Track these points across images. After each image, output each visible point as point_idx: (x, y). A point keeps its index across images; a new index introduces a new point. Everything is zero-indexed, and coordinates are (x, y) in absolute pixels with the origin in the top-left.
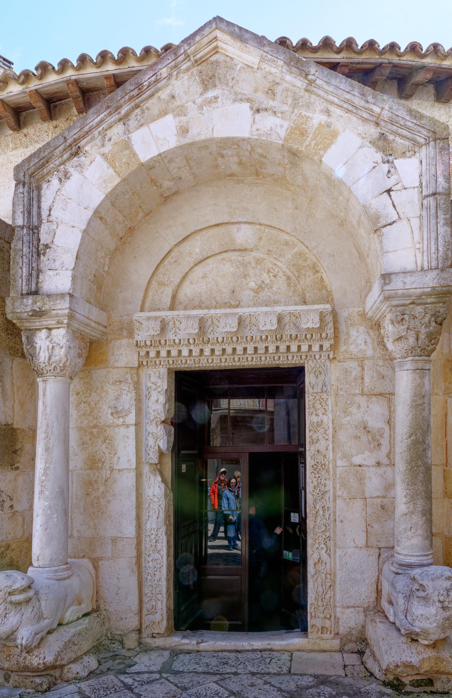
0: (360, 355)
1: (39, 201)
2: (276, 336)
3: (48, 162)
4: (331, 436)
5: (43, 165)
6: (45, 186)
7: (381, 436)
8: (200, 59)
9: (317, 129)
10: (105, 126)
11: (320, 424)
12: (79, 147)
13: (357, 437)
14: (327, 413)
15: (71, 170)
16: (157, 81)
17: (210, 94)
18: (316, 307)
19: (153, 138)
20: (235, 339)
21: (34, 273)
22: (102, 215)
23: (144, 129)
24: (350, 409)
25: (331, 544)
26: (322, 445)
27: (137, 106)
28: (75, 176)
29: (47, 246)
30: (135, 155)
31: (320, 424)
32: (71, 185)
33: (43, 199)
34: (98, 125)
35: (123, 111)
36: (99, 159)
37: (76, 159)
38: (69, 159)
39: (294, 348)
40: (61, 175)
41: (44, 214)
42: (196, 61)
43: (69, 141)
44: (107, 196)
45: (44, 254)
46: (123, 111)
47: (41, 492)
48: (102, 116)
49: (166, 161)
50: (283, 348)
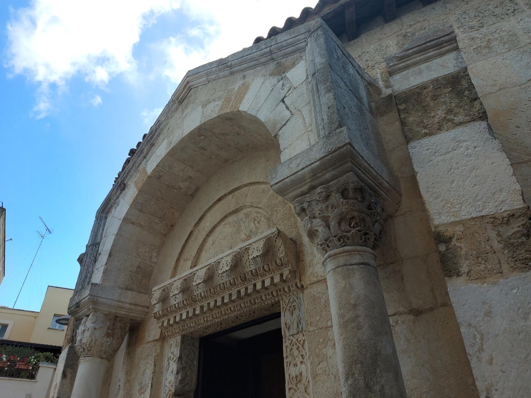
1: (104, 226)
2: (241, 276)
3: (110, 200)
8: (181, 99)
10: (136, 165)
11: (299, 378)
12: (125, 184)
14: (305, 360)
21: (89, 275)
22: (133, 220)
24: (324, 350)
31: (299, 378)
33: (106, 224)
34: (133, 166)
38: (121, 193)
42: (179, 102)
44: (131, 206)
49: (167, 169)
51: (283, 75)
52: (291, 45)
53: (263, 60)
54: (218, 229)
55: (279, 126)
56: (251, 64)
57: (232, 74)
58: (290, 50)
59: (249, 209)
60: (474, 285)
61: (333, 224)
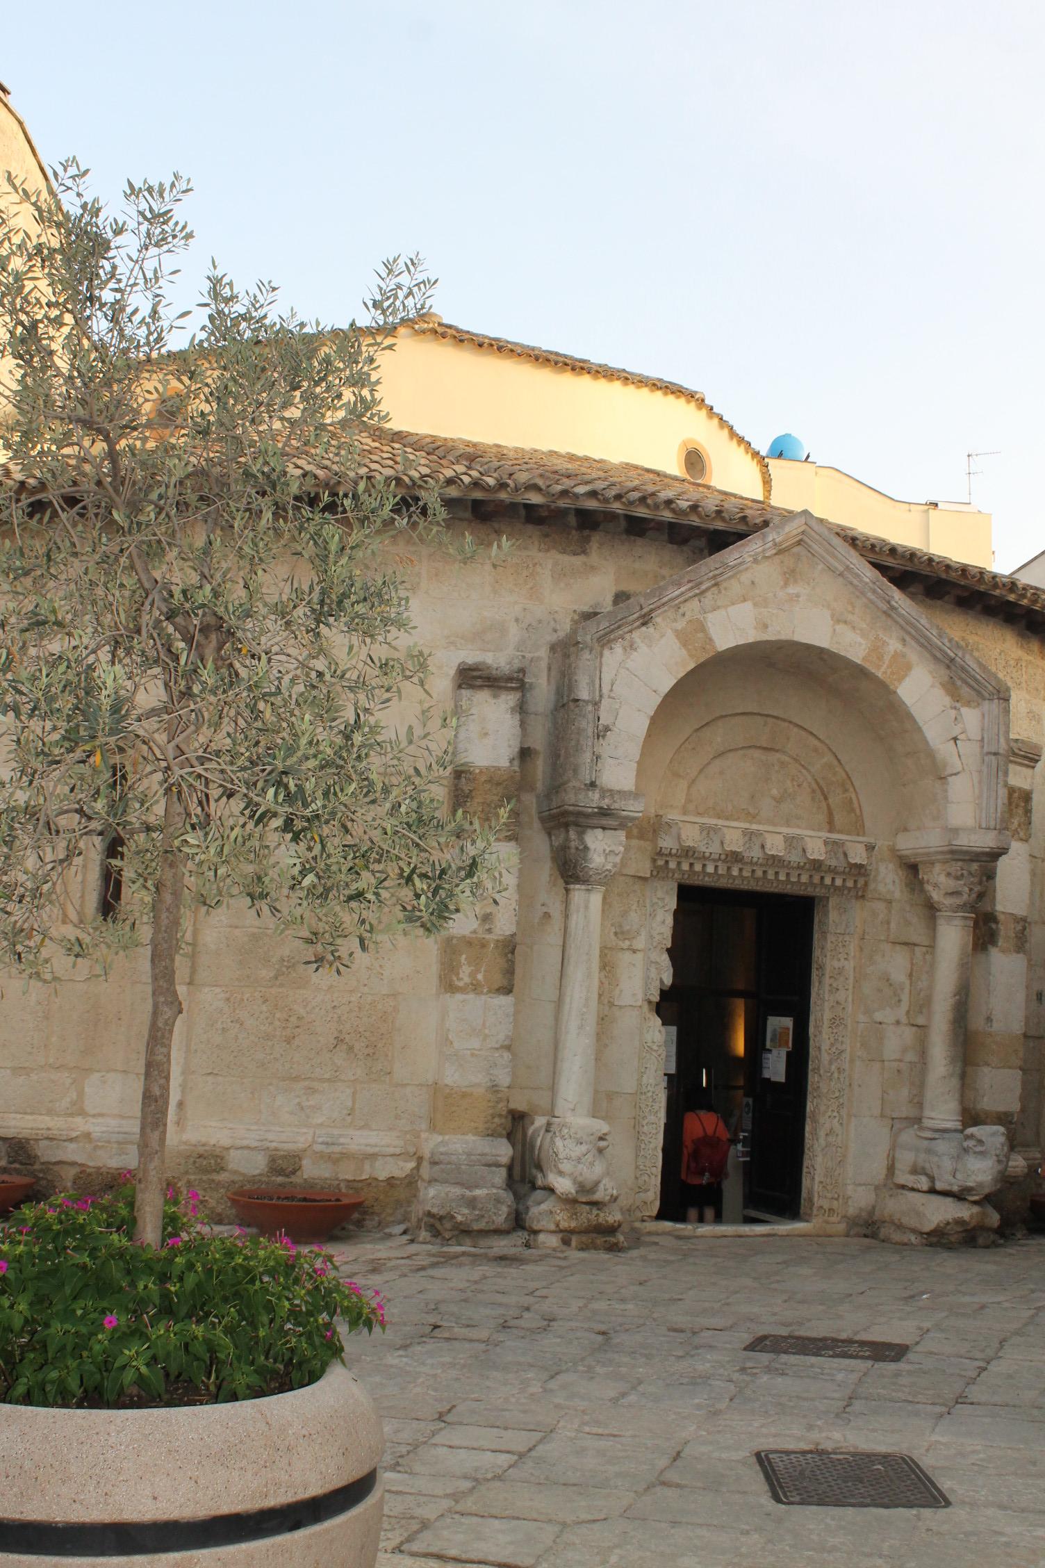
0: (888, 897)
3: (619, 627)
4: (851, 987)
5: (612, 631)
6: (606, 652)
7: (902, 989)
9: (893, 657)
11: (841, 971)
13: (880, 991)
15: (638, 640)
16: (740, 564)
17: (792, 590)
18: (861, 839)
19: (733, 624)
20: (770, 862)
23: (722, 612)
25: (844, 1112)
26: (841, 996)
27: (716, 584)
28: (643, 648)
29: (607, 729)
30: (711, 640)
31: (841, 971)
32: (638, 659)
33: (604, 669)
35: (703, 587)
36: (670, 634)
37: (644, 629)
38: (639, 627)
39: (828, 881)
40: (626, 643)
41: (605, 691)
43: (645, 611)
45: (604, 737)
46: (703, 587)
47: (581, 1027)
48: (683, 589)
50: (816, 880)
51: (958, 705)
52: (976, 680)
53: (938, 655)
54: (731, 755)
55: (949, 771)
56: (922, 640)
57: (884, 612)
58: (972, 683)
59: (787, 759)
60: (1001, 954)
61: (974, 896)
